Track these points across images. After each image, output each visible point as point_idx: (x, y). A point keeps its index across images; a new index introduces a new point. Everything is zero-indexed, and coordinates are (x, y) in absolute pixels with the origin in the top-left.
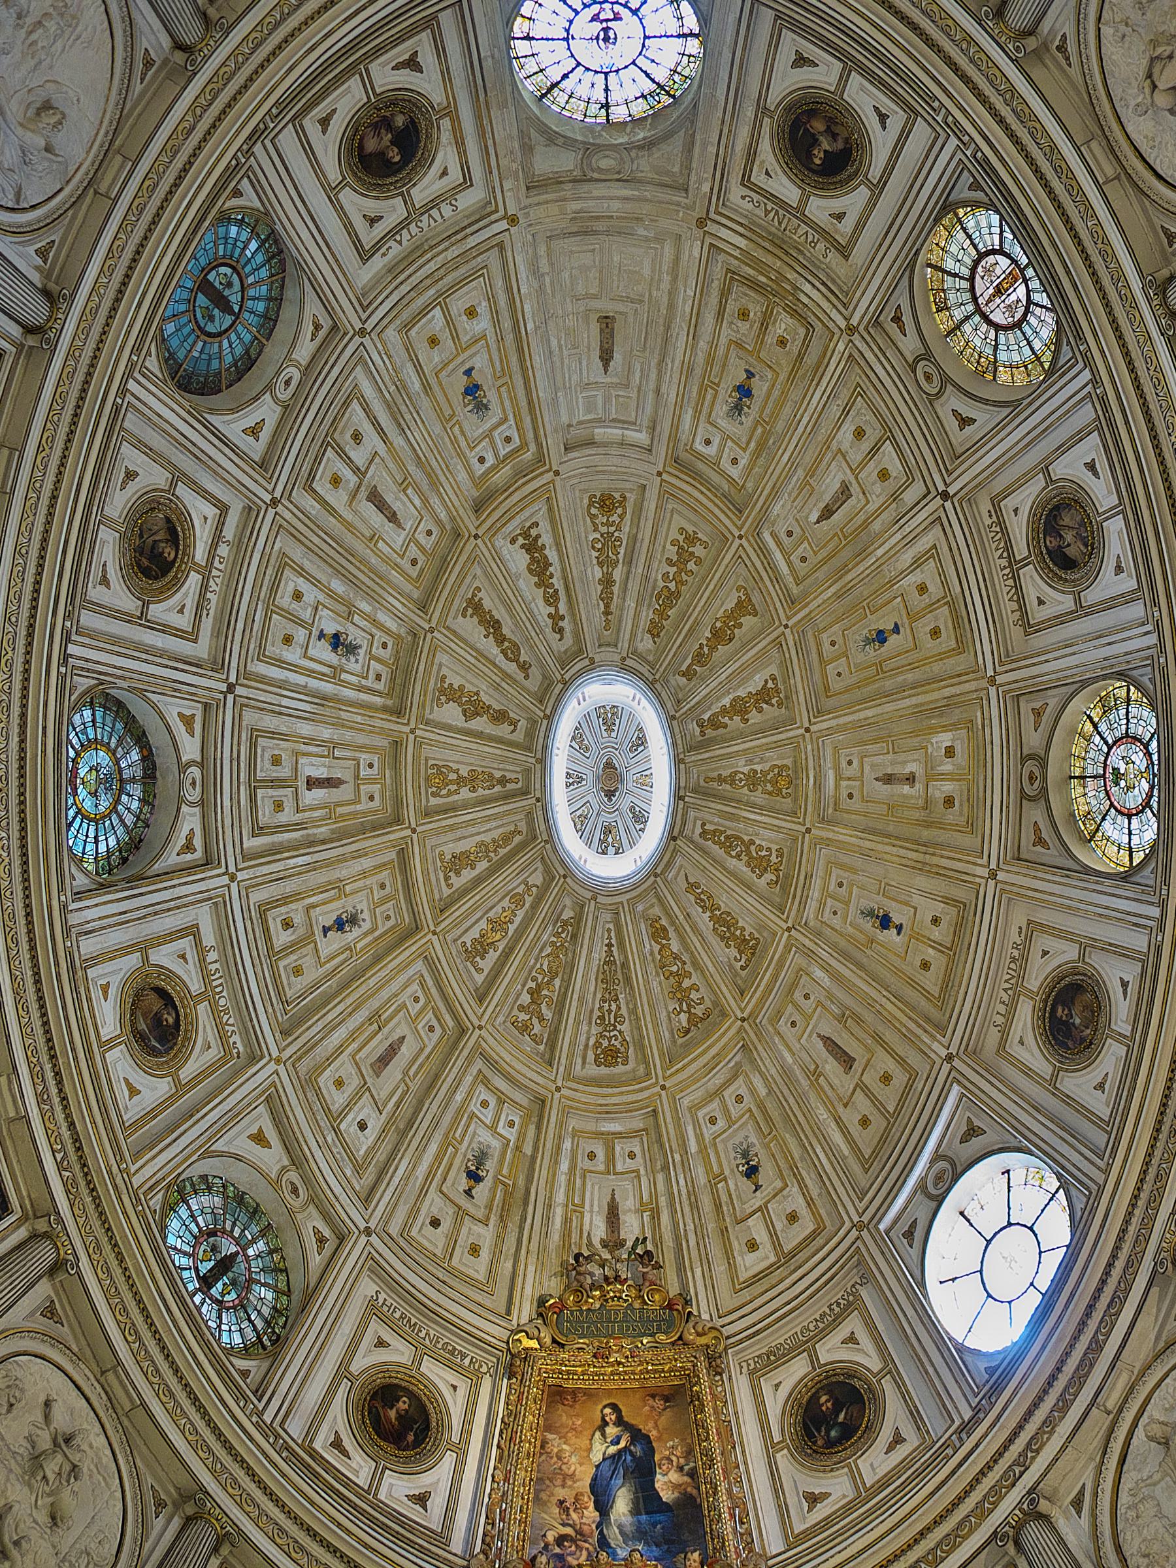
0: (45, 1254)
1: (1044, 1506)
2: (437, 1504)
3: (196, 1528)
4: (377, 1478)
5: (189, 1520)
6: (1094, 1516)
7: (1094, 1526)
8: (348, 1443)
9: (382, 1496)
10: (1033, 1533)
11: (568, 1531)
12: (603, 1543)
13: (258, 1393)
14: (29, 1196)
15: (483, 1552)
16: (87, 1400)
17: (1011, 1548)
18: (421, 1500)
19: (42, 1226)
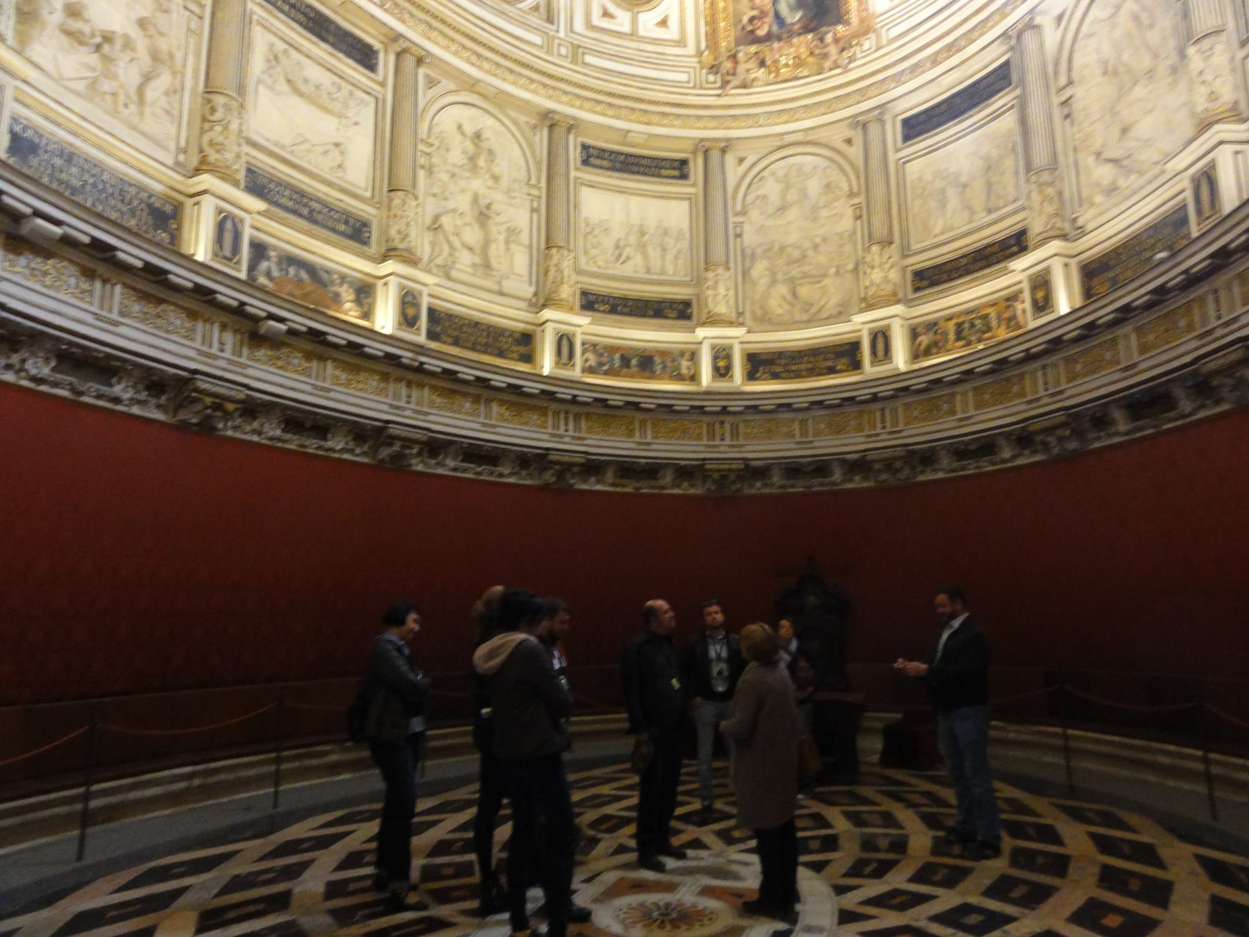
0: (409, 61)
1: (1038, 20)
2: (673, 22)
3: (557, 130)
4: (634, 22)
5: (551, 127)
6: (1066, 29)
7: (1062, 43)
8: (612, 9)
9: (642, 32)
10: (1028, 37)
11: (755, 13)
12: (777, 16)
13: (550, 20)
14: (380, 33)
15: (707, 47)
16: (473, 105)
17: (1013, 42)
18: (663, 23)
19: (397, 47)
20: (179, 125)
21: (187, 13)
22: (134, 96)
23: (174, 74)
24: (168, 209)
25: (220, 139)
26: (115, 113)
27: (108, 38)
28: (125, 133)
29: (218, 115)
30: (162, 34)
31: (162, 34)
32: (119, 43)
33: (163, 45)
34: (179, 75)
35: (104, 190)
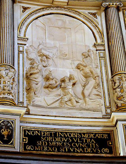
20: (105, 97)
21: (98, 51)
22: (81, 97)
23: (95, 78)
24: (105, 136)
25: (120, 94)
26: (73, 108)
27: (63, 81)
28: (78, 114)
29: (117, 84)
30: (85, 66)
31: (85, 66)
32: (67, 81)
33: (87, 70)
34: (97, 77)
35: (73, 141)
